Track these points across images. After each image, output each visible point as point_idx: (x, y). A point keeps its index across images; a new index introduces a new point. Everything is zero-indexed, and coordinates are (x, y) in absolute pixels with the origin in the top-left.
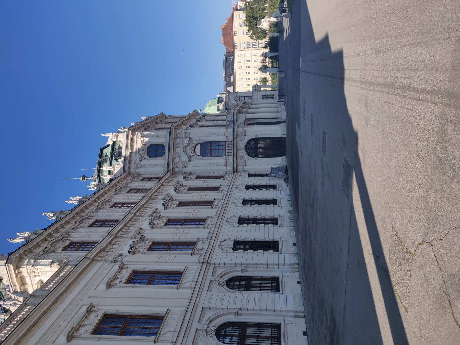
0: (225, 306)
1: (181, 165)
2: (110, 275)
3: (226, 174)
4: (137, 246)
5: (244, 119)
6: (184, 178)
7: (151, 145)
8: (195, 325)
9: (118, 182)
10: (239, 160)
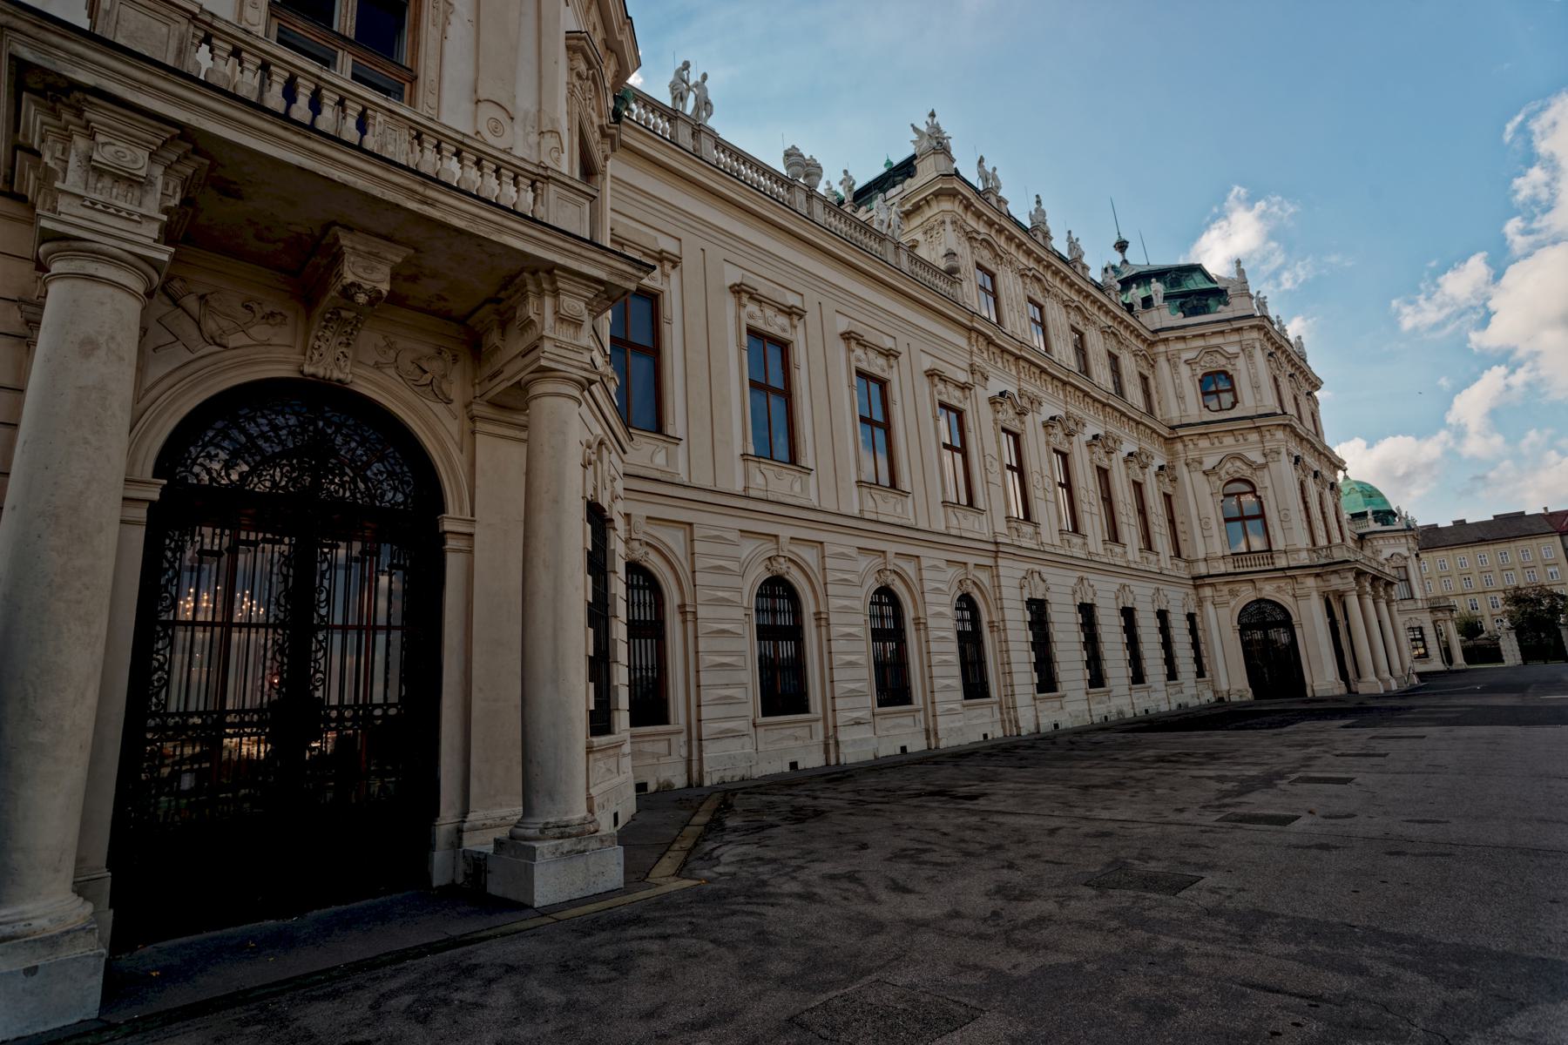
0: (928, 597)
1: (1193, 454)
2: (949, 372)
3: (1186, 561)
4: (1007, 406)
5: (1341, 588)
6: (1161, 468)
7: (1229, 378)
8: (891, 548)
9: (1128, 326)
10: (1225, 589)
